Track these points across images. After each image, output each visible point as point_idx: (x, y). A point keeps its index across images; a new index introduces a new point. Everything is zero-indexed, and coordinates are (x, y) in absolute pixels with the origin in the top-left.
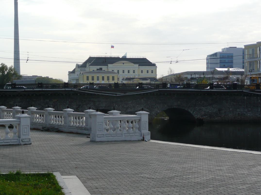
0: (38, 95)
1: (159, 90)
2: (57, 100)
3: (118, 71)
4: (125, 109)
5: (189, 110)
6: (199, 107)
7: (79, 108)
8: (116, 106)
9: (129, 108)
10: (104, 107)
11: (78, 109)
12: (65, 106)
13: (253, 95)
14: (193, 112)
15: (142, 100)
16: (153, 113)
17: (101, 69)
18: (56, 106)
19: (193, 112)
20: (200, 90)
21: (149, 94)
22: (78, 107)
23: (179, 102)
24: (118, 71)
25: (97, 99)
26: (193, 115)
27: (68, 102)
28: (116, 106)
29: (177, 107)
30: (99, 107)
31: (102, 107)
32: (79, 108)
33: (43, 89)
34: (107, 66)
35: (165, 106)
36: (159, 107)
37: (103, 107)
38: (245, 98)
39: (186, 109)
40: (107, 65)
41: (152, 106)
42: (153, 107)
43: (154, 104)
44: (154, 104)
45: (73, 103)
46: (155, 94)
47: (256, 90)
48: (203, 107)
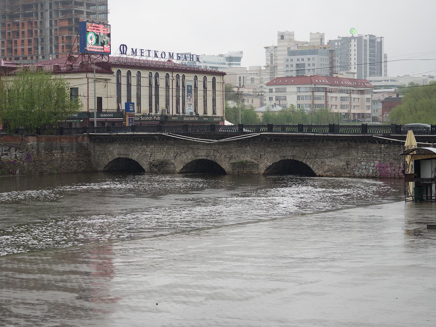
1: (260, 134)
2: (154, 147)
4: (228, 160)
5: (308, 163)
6: (321, 158)
8: (218, 155)
9: (233, 159)
10: (203, 156)
11: (177, 158)
12: (163, 154)
13: (392, 142)
15: (248, 148)
16: (262, 166)
18: (154, 153)
19: (314, 165)
22: (176, 156)
26: (313, 170)
27: (165, 149)
28: (218, 155)
29: (292, 159)
30: (199, 156)
31: (201, 156)
32: (176, 157)
37: (202, 156)
39: (304, 162)
41: (261, 156)
43: (263, 154)
44: (263, 154)
45: (170, 151)
47: (392, 135)
48: (327, 158)
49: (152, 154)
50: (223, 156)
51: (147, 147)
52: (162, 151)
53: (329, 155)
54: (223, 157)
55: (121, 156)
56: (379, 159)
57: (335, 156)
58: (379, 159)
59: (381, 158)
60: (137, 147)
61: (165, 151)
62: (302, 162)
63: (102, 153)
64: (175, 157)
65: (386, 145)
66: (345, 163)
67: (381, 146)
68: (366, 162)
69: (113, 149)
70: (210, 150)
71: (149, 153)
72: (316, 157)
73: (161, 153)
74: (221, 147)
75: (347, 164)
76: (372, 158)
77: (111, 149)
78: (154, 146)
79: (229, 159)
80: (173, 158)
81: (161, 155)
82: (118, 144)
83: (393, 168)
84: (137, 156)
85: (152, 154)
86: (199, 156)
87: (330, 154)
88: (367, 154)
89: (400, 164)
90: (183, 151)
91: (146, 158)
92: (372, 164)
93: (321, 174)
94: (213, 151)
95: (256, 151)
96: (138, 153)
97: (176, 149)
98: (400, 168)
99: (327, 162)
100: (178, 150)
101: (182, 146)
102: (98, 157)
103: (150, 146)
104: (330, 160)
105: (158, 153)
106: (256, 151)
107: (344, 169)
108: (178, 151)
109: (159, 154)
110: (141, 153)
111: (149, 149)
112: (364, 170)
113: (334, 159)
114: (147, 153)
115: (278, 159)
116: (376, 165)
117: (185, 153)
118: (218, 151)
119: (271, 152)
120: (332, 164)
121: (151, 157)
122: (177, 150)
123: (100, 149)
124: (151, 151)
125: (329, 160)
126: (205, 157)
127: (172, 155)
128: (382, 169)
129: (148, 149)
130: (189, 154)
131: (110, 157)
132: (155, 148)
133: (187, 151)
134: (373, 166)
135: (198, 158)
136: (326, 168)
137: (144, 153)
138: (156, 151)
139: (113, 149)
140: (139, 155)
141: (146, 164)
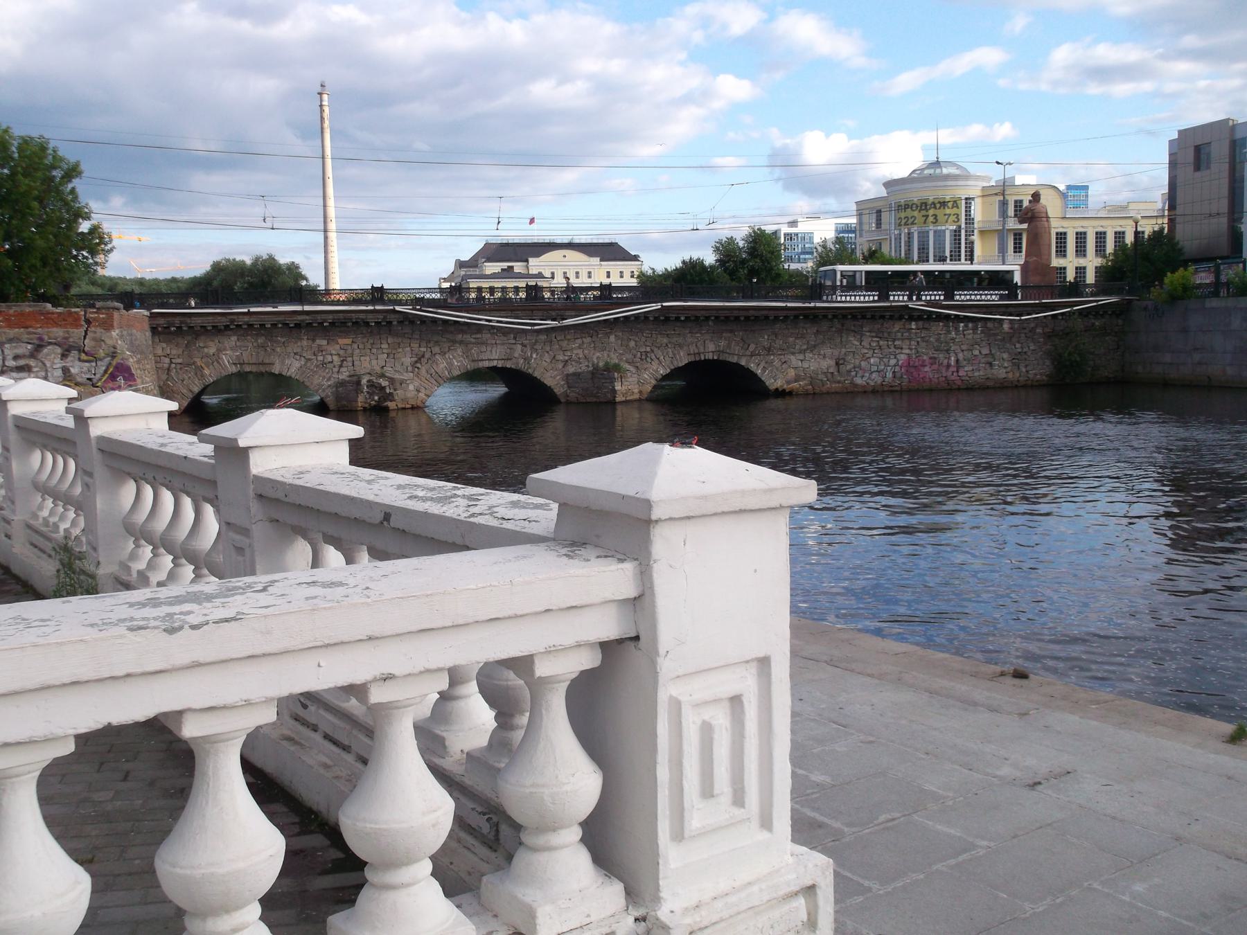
0: (291, 325)
3: (553, 274)
7: (419, 365)
11: (418, 368)
14: (764, 369)
15: (612, 338)
17: (511, 268)
18: (349, 359)
19: (764, 369)
20: (784, 305)
21: (633, 318)
22: (416, 362)
23: (723, 343)
24: (553, 274)
25: (474, 336)
26: (763, 379)
27: (385, 346)
28: (534, 356)
29: (715, 358)
30: (482, 360)
31: (489, 360)
32: (419, 365)
33: (307, 308)
34: (525, 264)
35: (682, 354)
36: (662, 358)
38: (914, 327)
39: (743, 363)
40: (527, 261)
42: (643, 357)
44: (648, 349)
45: (400, 350)
46: (651, 319)
48: (793, 354)
49: (342, 361)
50: (547, 358)
51: (328, 343)
52: (374, 351)
53: (797, 347)
54: (548, 360)
55: (248, 369)
56: (907, 351)
57: (812, 348)
58: (907, 351)
59: (911, 349)
60: (299, 344)
61: (384, 351)
62: (737, 365)
63: (180, 361)
64: (413, 365)
65: (920, 323)
66: (832, 363)
67: (910, 324)
68: (880, 358)
69: (219, 350)
70: (514, 346)
71: (336, 358)
72: (769, 350)
73: (373, 357)
74: (543, 337)
75: (837, 364)
76: (892, 349)
77: (212, 351)
78: (351, 340)
79: (562, 364)
80: (410, 369)
81: (374, 362)
82: (234, 338)
83: (935, 367)
84: (299, 365)
85: (342, 361)
86: (482, 360)
87: (800, 344)
88: (881, 343)
89: (949, 358)
90: (436, 349)
91: (327, 371)
92: (893, 362)
93: (781, 386)
94: (519, 347)
95: (632, 344)
96: (303, 358)
97: (418, 345)
98: (949, 366)
99: (794, 360)
100: (422, 349)
101: (436, 338)
102: (168, 374)
103: (341, 341)
104: (801, 357)
105: (365, 358)
106: (632, 344)
107: (829, 375)
108: (425, 350)
109: (368, 358)
110: (310, 360)
111: (338, 347)
112: (874, 375)
113: (809, 355)
114: (329, 358)
115: (683, 359)
116: (900, 363)
117: (443, 354)
118: (535, 347)
119: (667, 345)
120: (806, 365)
121: (341, 366)
122: (420, 346)
123: (174, 352)
124: (342, 352)
125: (799, 358)
126: (499, 362)
127: (408, 360)
128: (912, 370)
129: (334, 349)
130: (454, 357)
131: (207, 372)
132: (355, 346)
133: (449, 350)
134: (895, 366)
135: (481, 365)
136: (792, 373)
137: (320, 358)
138: (358, 351)
139: (219, 350)
140: (306, 363)
141: (329, 386)
